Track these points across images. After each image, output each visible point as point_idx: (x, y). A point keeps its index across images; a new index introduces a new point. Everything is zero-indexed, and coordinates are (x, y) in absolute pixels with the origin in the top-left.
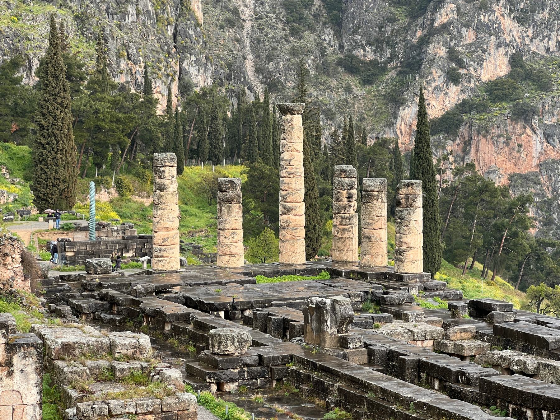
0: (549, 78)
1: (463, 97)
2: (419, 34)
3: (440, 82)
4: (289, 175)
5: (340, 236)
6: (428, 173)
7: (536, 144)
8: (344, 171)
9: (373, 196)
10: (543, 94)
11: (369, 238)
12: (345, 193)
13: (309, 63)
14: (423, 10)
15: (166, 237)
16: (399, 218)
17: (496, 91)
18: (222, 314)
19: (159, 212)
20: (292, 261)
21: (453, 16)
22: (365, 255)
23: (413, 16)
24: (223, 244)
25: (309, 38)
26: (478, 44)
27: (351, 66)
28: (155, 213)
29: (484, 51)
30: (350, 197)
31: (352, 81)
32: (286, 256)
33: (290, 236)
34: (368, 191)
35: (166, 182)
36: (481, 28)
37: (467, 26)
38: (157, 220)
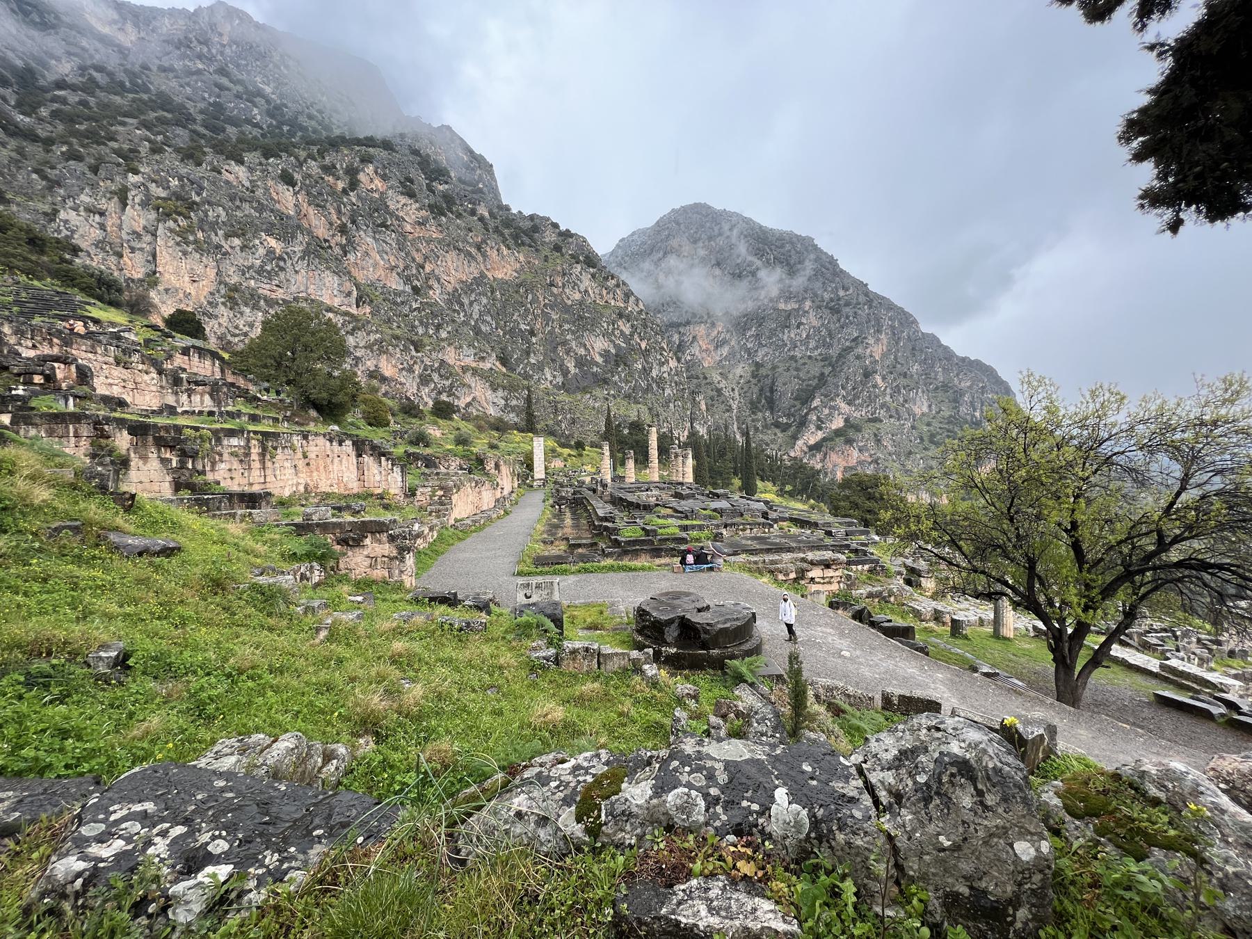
7: (855, 453)
13: (759, 425)
17: (838, 433)
23: (803, 404)
25: (760, 414)
26: (830, 414)
27: (777, 425)
31: (777, 431)
36: (831, 408)
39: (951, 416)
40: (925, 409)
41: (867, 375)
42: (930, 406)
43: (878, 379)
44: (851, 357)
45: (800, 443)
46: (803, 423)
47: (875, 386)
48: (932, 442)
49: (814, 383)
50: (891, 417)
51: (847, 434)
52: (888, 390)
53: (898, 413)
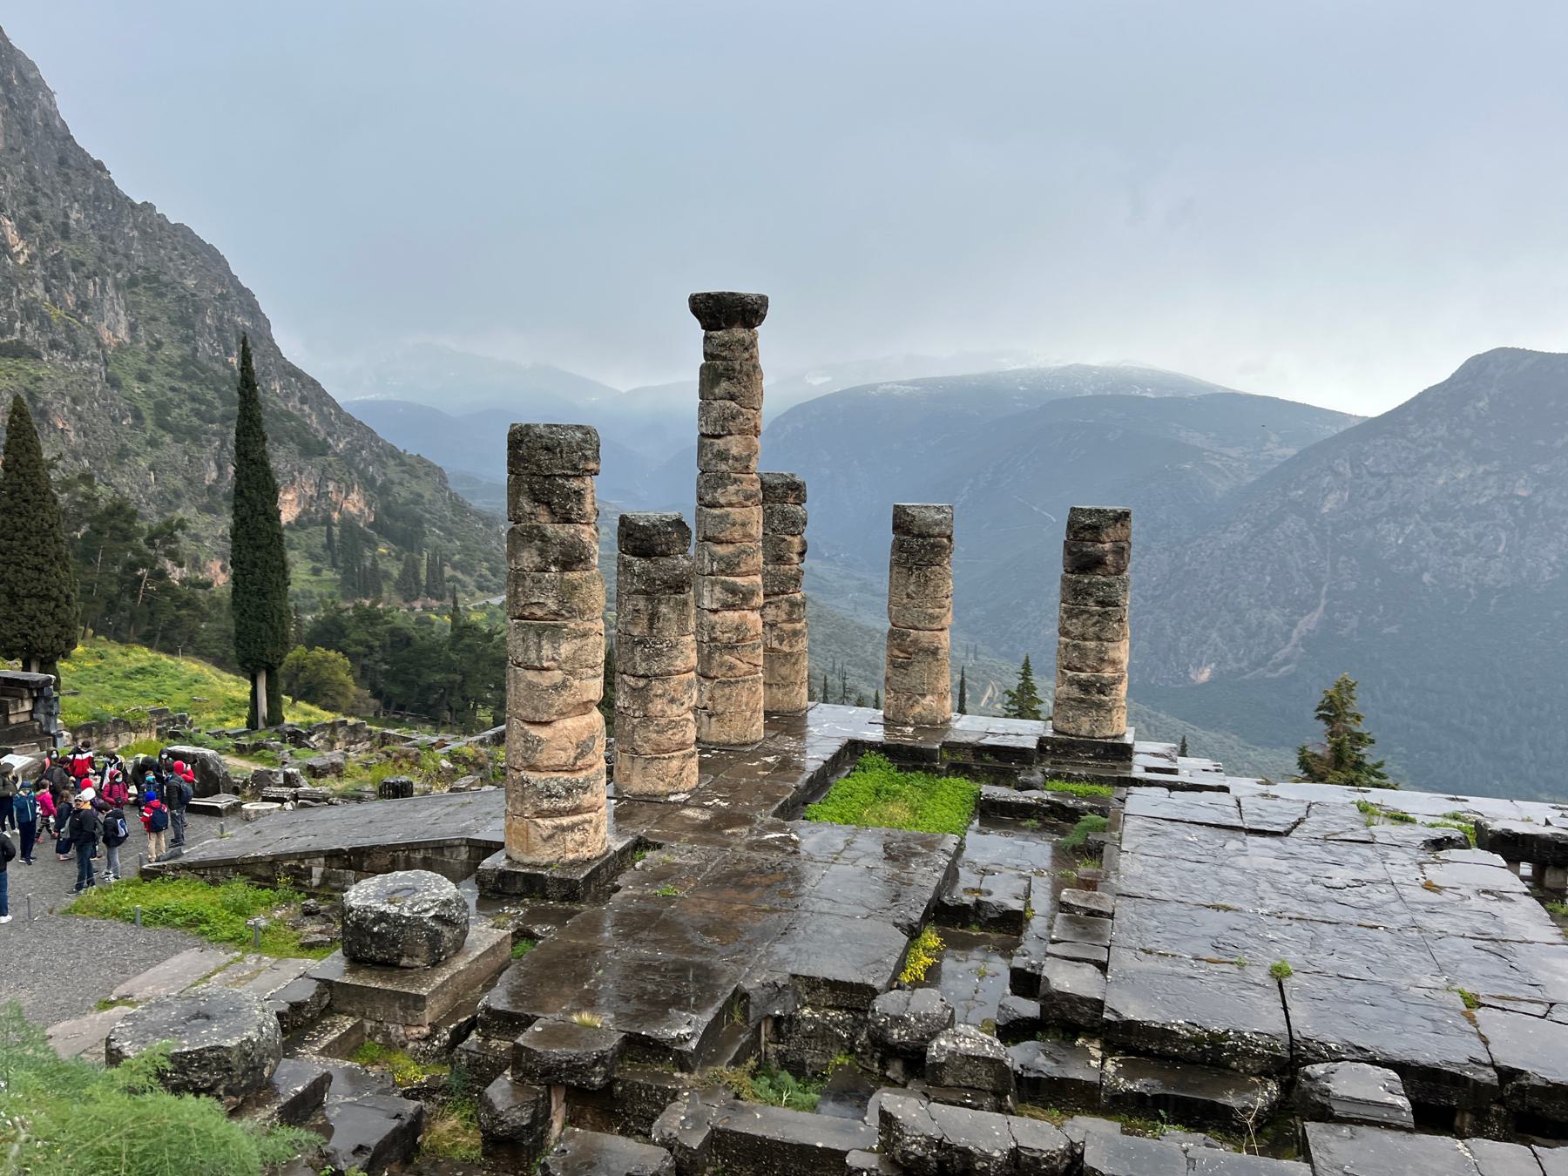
4: (747, 499)
5: (787, 649)
6: (268, 489)
9: (943, 547)
11: (934, 652)
12: (796, 540)
15: (585, 737)
16: (1102, 603)
19: (566, 649)
22: (923, 696)
24: (663, 721)
28: (547, 650)
32: (738, 723)
33: (745, 667)
34: (930, 536)
38: (558, 676)
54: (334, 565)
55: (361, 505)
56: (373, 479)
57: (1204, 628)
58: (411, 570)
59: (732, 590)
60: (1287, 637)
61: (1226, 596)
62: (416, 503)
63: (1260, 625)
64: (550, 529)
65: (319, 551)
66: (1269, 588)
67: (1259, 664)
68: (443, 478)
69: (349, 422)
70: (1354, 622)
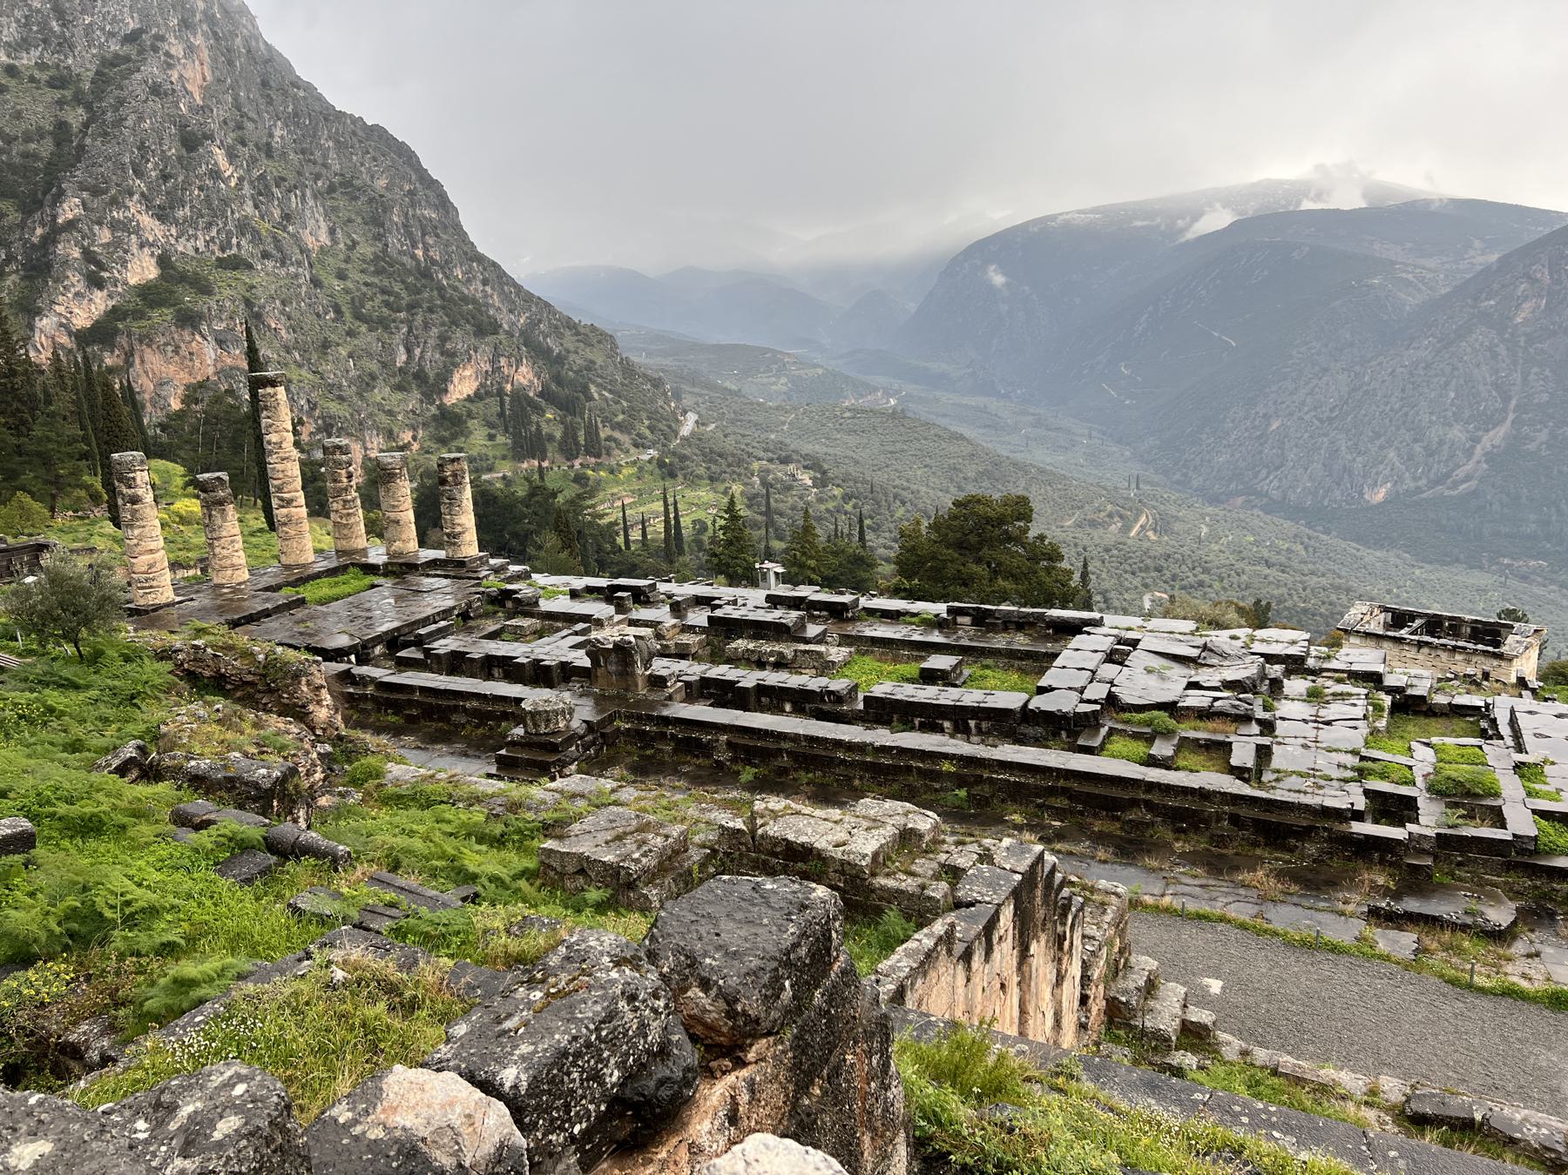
0: (207, 280)
1: (111, 303)
2: (39, 231)
3: (80, 287)
7: (210, 351)
8: (339, 447)
10: (205, 298)
11: (398, 522)
14: (39, 204)
17: (150, 295)
18: (353, 658)
19: (136, 532)
20: (302, 561)
21: (79, 211)
26: (116, 244)
29: (126, 252)
30: (350, 476)
35: (140, 492)
36: (115, 226)
37: (100, 223)
39: (377, 257)
40: (324, 239)
41: (191, 142)
42: (332, 232)
43: (220, 156)
44: (136, 85)
45: (46, 323)
46: (40, 269)
47: (216, 174)
48: (358, 317)
49: (46, 148)
50: (266, 255)
51: (174, 296)
52: (247, 190)
53: (279, 249)
54: (506, 431)
55: (530, 376)
56: (550, 350)
57: (1381, 448)
58: (570, 433)
59: (282, 499)
60: (1469, 453)
61: (1406, 414)
62: (588, 369)
63: (1441, 443)
64: (125, 491)
65: (494, 419)
66: (1452, 404)
67: (1437, 482)
68: (614, 346)
69: (529, 298)
70: (1544, 436)
